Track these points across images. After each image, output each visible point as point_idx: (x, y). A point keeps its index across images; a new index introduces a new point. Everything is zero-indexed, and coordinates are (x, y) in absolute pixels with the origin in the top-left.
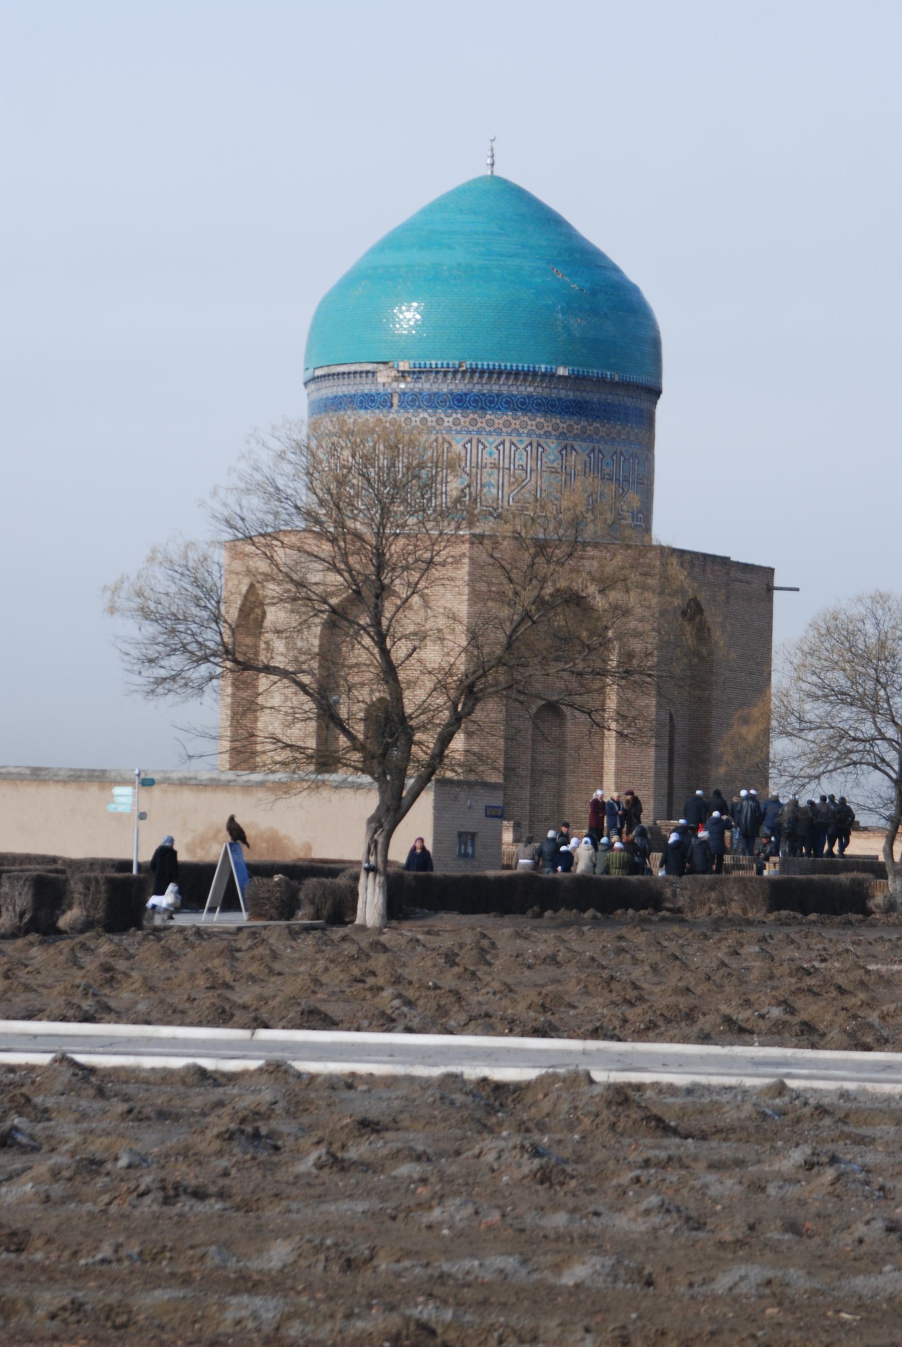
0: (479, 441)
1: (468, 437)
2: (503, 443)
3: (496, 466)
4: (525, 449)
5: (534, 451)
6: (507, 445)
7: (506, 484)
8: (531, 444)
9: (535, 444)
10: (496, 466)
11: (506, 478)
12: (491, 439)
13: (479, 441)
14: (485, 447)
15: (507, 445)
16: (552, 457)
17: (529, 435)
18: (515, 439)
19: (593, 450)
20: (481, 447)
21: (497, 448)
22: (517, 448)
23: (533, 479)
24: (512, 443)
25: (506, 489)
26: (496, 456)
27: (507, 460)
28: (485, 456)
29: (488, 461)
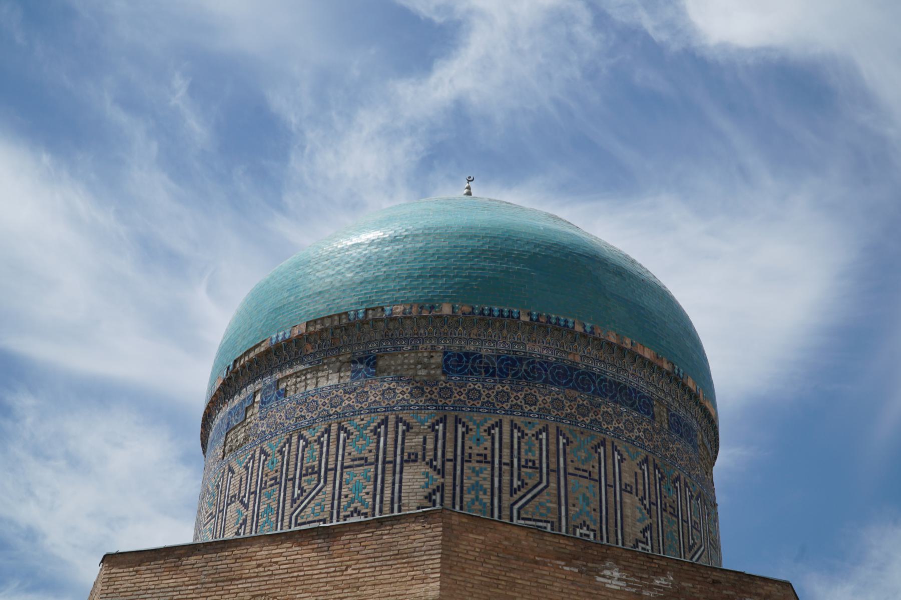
0: (457, 421)
1: (441, 414)
2: (499, 424)
3: (484, 459)
4: (537, 435)
5: (553, 440)
6: (506, 428)
7: (506, 489)
8: (545, 429)
9: (552, 430)
10: (484, 459)
11: (506, 478)
12: (477, 417)
13: (457, 421)
14: (468, 430)
15: (506, 428)
16: (583, 455)
17: (543, 413)
18: (519, 421)
19: (646, 460)
20: (461, 429)
21: (488, 431)
22: (524, 434)
23: (553, 485)
24: (513, 426)
25: (506, 496)
26: (488, 444)
27: (506, 452)
28: (468, 443)
29: (476, 450)
